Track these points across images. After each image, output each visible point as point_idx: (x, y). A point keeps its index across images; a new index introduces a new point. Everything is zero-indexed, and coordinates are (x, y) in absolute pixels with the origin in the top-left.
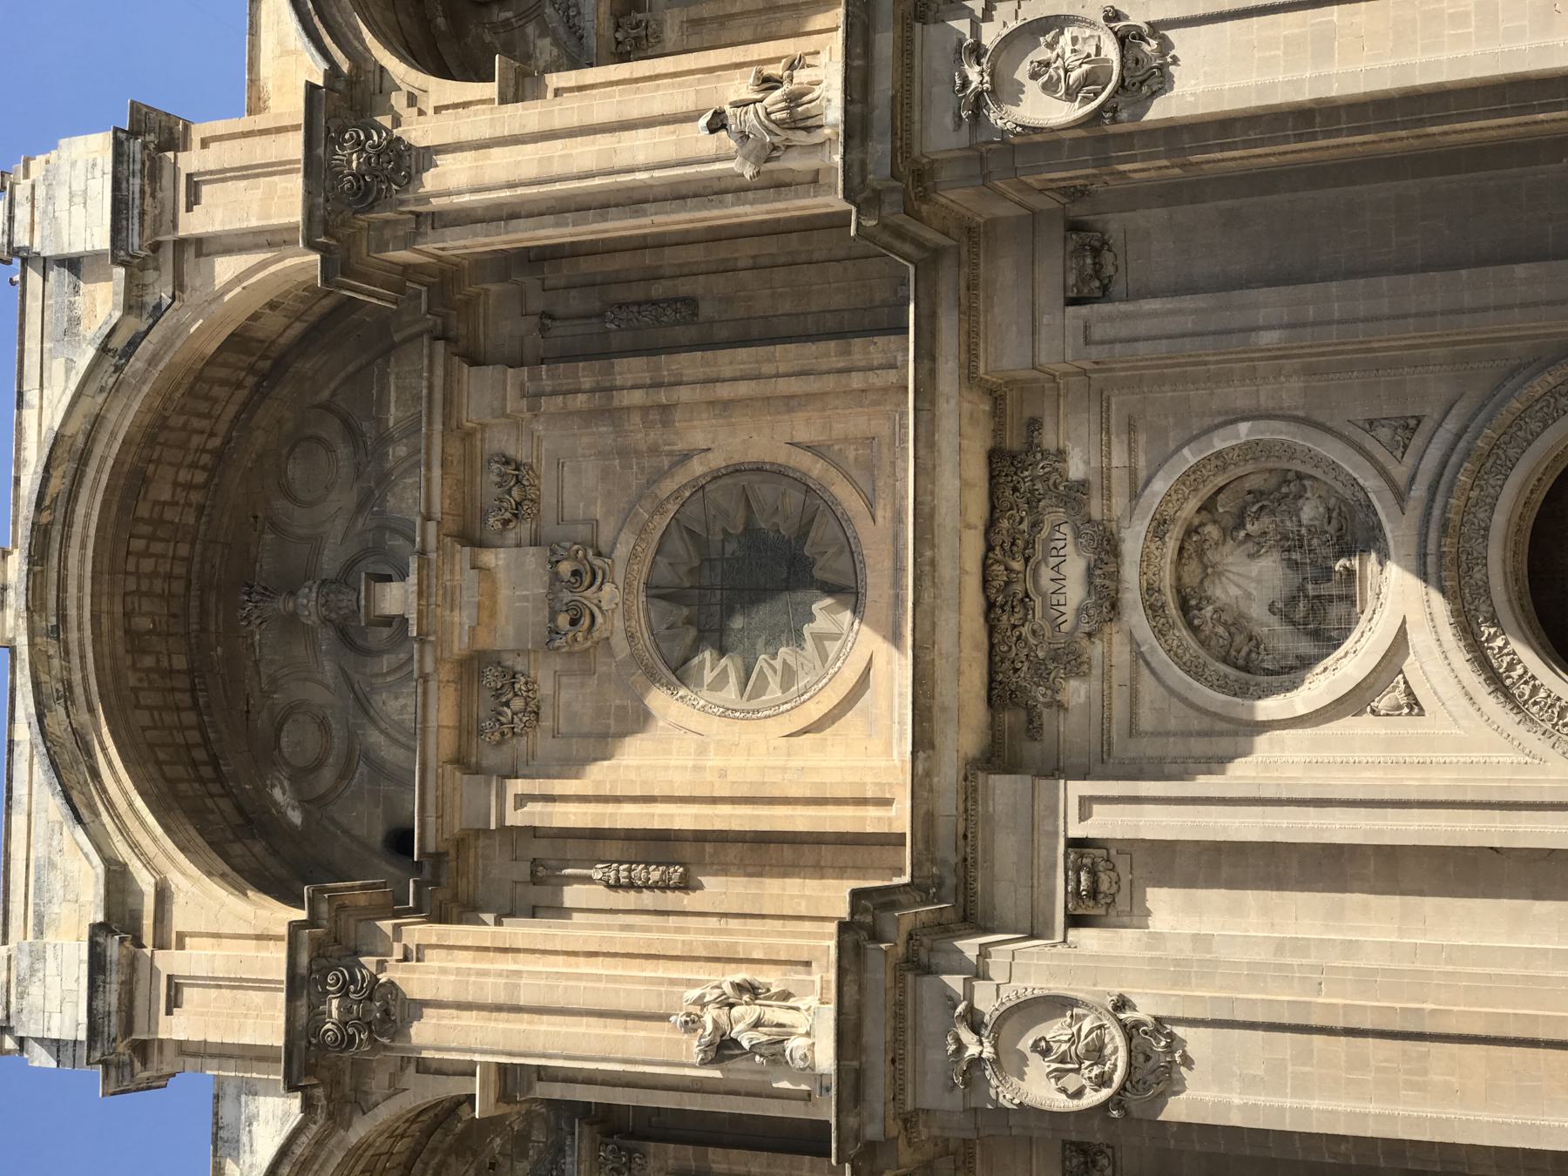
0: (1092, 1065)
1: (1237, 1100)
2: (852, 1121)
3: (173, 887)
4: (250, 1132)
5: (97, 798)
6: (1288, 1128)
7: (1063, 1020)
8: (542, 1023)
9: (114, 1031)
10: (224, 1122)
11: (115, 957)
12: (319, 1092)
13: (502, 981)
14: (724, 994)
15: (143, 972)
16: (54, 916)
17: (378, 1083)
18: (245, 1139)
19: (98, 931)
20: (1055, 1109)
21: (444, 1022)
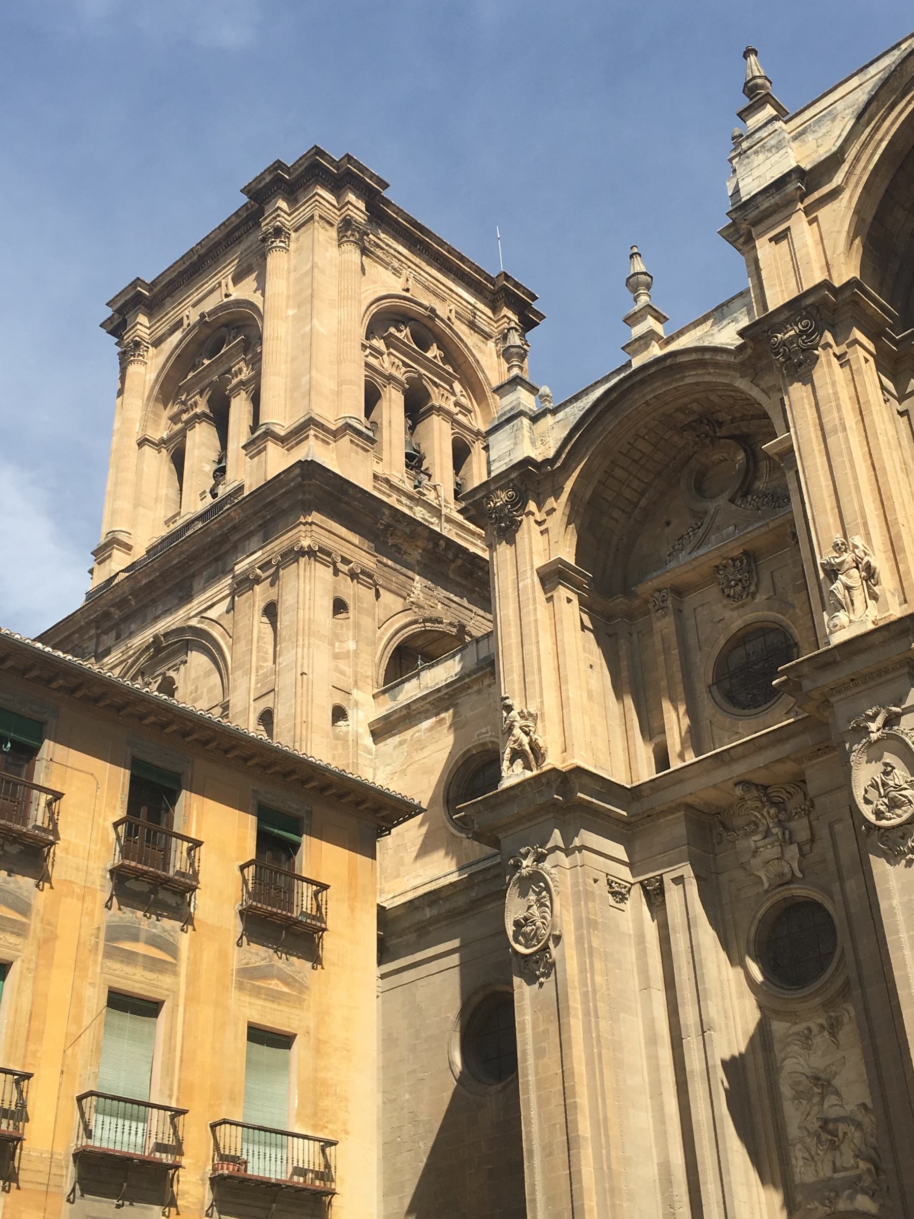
0: (886, 804)
1: (895, 902)
2: (806, 669)
3: (841, 196)
4: (729, 323)
5: (877, 118)
6: (888, 939)
7: (909, 776)
8: (822, 458)
9: (750, 216)
10: (731, 305)
11: (788, 191)
12: (749, 351)
13: (837, 422)
14: (862, 559)
15: (786, 213)
16: (806, 139)
17: (768, 380)
18: (725, 322)
19: (798, 171)
20: (854, 790)
21: (806, 401)
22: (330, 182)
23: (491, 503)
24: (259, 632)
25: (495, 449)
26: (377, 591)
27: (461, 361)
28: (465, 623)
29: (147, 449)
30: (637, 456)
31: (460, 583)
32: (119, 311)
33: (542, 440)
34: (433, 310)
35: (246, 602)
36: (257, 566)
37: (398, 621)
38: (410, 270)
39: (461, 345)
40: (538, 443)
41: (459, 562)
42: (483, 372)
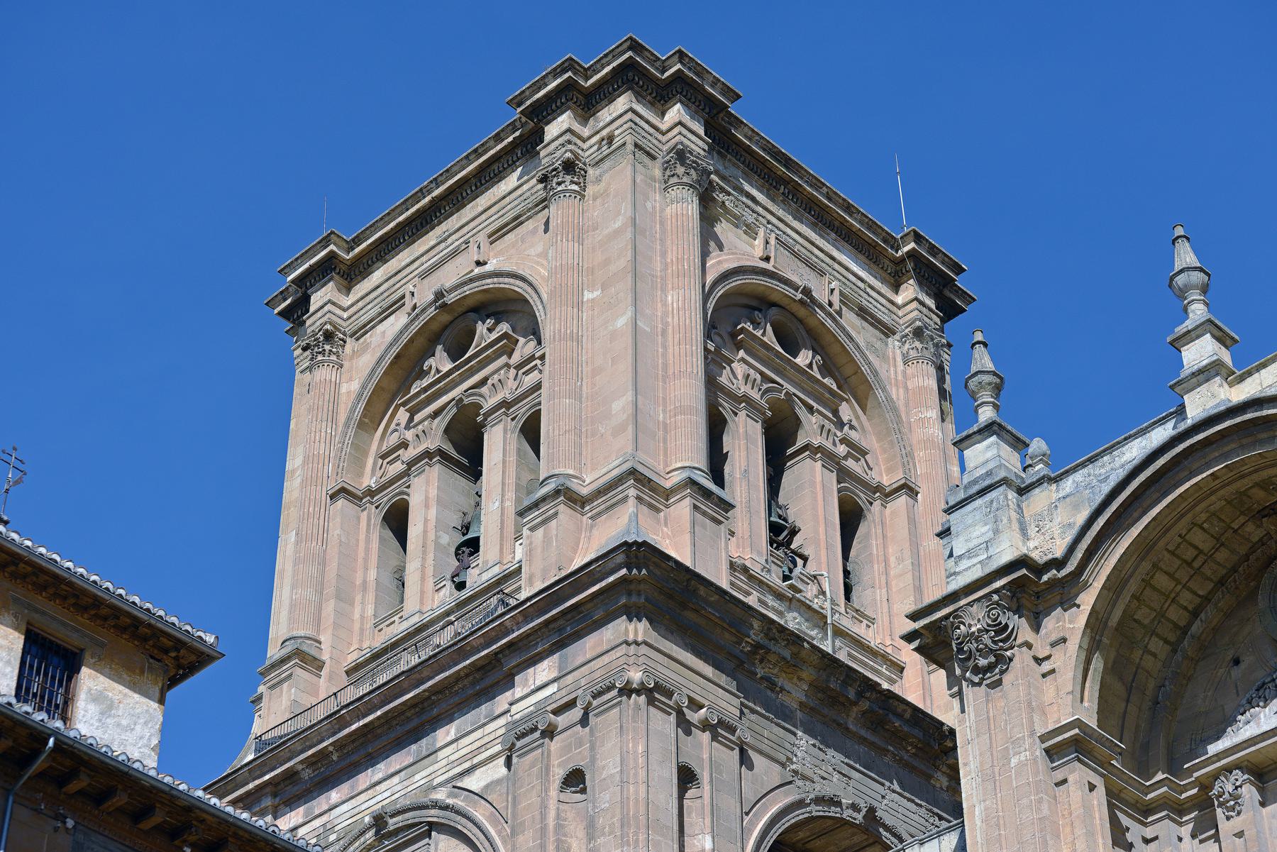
22: (650, 91)
23: (962, 627)
24: (558, 816)
25: (961, 539)
26: (743, 752)
27: (848, 370)
28: (875, 804)
29: (341, 503)
30: (1189, 554)
31: (865, 739)
32: (299, 281)
33: (1037, 526)
34: (807, 292)
35: (533, 765)
36: (549, 708)
37: (774, 802)
38: (769, 226)
39: (850, 347)
40: (1032, 531)
41: (865, 705)
42: (884, 389)
